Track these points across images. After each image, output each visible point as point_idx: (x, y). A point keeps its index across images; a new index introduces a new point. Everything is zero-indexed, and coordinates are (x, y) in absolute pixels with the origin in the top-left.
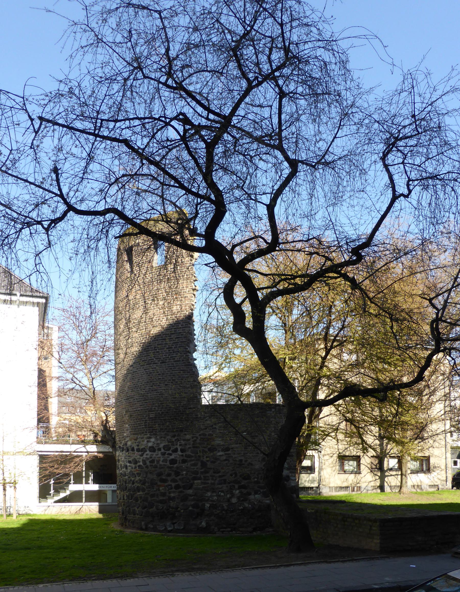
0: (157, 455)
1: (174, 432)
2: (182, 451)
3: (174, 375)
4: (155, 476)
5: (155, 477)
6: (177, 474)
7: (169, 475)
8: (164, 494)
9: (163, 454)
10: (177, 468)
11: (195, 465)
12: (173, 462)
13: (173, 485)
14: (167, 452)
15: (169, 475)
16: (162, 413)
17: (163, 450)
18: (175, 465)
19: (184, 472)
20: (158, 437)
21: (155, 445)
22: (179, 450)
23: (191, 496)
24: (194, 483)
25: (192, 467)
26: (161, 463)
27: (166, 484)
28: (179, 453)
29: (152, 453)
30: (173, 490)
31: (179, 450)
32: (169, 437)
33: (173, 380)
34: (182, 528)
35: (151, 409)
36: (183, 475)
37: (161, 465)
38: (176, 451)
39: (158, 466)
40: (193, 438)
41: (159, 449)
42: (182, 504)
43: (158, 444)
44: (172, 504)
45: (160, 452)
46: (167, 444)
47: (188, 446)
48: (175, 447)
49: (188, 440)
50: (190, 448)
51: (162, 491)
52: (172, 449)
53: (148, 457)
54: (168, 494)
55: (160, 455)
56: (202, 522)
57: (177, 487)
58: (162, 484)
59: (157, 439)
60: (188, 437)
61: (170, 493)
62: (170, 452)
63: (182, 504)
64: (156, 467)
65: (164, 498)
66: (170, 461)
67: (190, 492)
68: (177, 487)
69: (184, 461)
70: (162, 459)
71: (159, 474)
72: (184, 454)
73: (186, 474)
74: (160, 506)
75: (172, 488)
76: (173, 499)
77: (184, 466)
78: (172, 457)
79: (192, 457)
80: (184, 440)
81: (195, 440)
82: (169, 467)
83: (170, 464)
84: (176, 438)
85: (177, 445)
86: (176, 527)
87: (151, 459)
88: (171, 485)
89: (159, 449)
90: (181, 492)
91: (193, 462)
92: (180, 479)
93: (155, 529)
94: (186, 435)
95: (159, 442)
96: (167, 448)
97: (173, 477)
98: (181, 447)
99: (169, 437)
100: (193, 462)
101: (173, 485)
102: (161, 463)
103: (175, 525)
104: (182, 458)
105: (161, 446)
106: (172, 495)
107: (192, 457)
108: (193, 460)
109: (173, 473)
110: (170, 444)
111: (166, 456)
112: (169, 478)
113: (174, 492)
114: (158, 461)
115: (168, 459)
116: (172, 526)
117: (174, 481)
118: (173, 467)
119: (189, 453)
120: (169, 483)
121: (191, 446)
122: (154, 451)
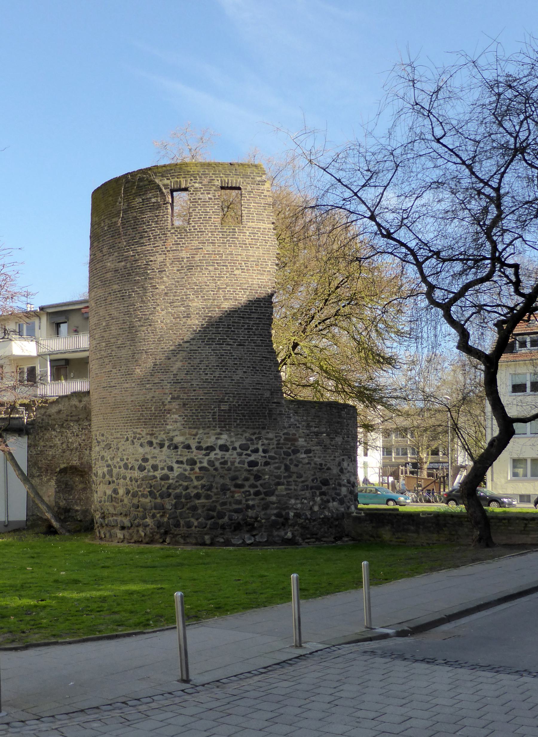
0: (232, 455)
1: (254, 428)
2: (265, 451)
3: (254, 362)
4: (228, 480)
5: (228, 481)
6: (257, 477)
7: (247, 479)
8: (239, 502)
9: (240, 454)
10: (258, 471)
11: (278, 468)
12: (253, 464)
13: (252, 491)
14: (245, 452)
15: (247, 479)
16: (239, 405)
17: (239, 450)
18: (255, 468)
19: (267, 477)
20: (232, 434)
21: (228, 444)
22: (261, 450)
23: (273, 503)
24: (277, 489)
25: (275, 471)
26: (236, 464)
27: (242, 490)
28: (261, 453)
29: (224, 453)
30: (252, 497)
31: (261, 450)
32: (247, 435)
33: (253, 367)
34: (266, 539)
35: (224, 399)
36: (264, 479)
37: (236, 467)
38: (256, 451)
39: (233, 468)
40: (276, 437)
41: (234, 449)
42: (263, 513)
43: (232, 442)
44: (250, 513)
45: (235, 452)
46: (244, 442)
47: (271, 447)
48: (255, 446)
49: (271, 439)
50: (273, 448)
51: (238, 498)
52: (250, 449)
53: (219, 457)
54: (244, 502)
55: (235, 455)
56: (287, 533)
57: (257, 494)
58: (237, 489)
59: (230, 437)
60: (270, 435)
61: (247, 500)
62: (249, 452)
63: (263, 513)
64: (229, 469)
65: (240, 506)
66: (248, 463)
67: (273, 499)
68: (257, 494)
69: (267, 464)
70: (238, 460)
71: (234, 479)
72: (267, 455)
73: (269, 478)
74: (235, 516)
75: (250, 495)
76: (252, 507)
77: (267, 469)
78: (252, 458)
79: (276, 458)
80: (267, 439)
81: (279, 440)
82: (246, 470)
83: (249, 466)
84: (256, 436)
85: (257, 444)
86: (258, 539)
87: (223, 460)
88: (249, 491)
89: (234, 449)
90: (263, 499)
91: (277, 465)
92: (261, 485)
93: (227, 543)
94: (268, 433)
95: (233, 439)
96: (244, 447)
97: (252, 481)
98: (263, 447)
99: (247, 435)
100: (277, 465)
101: (252, 491)
102: (236, 464)
103: (257, 537)
104: (264, 460)
105: (237, 445)
106: (251, 503)
107: (276, 458)
108: (277, 463)
109: (252, 478)
110: (249, 442)
111: (244, 456)
112: (247, 484)
113: (253, 499)
114: (233, 463)
115: (246, 461)
116: (253, 538)
117: (253, 486)
118: (252, 470)
119: (272, 454)
120: (247, 488)
121: (275, 446)
122: (227, 450)
